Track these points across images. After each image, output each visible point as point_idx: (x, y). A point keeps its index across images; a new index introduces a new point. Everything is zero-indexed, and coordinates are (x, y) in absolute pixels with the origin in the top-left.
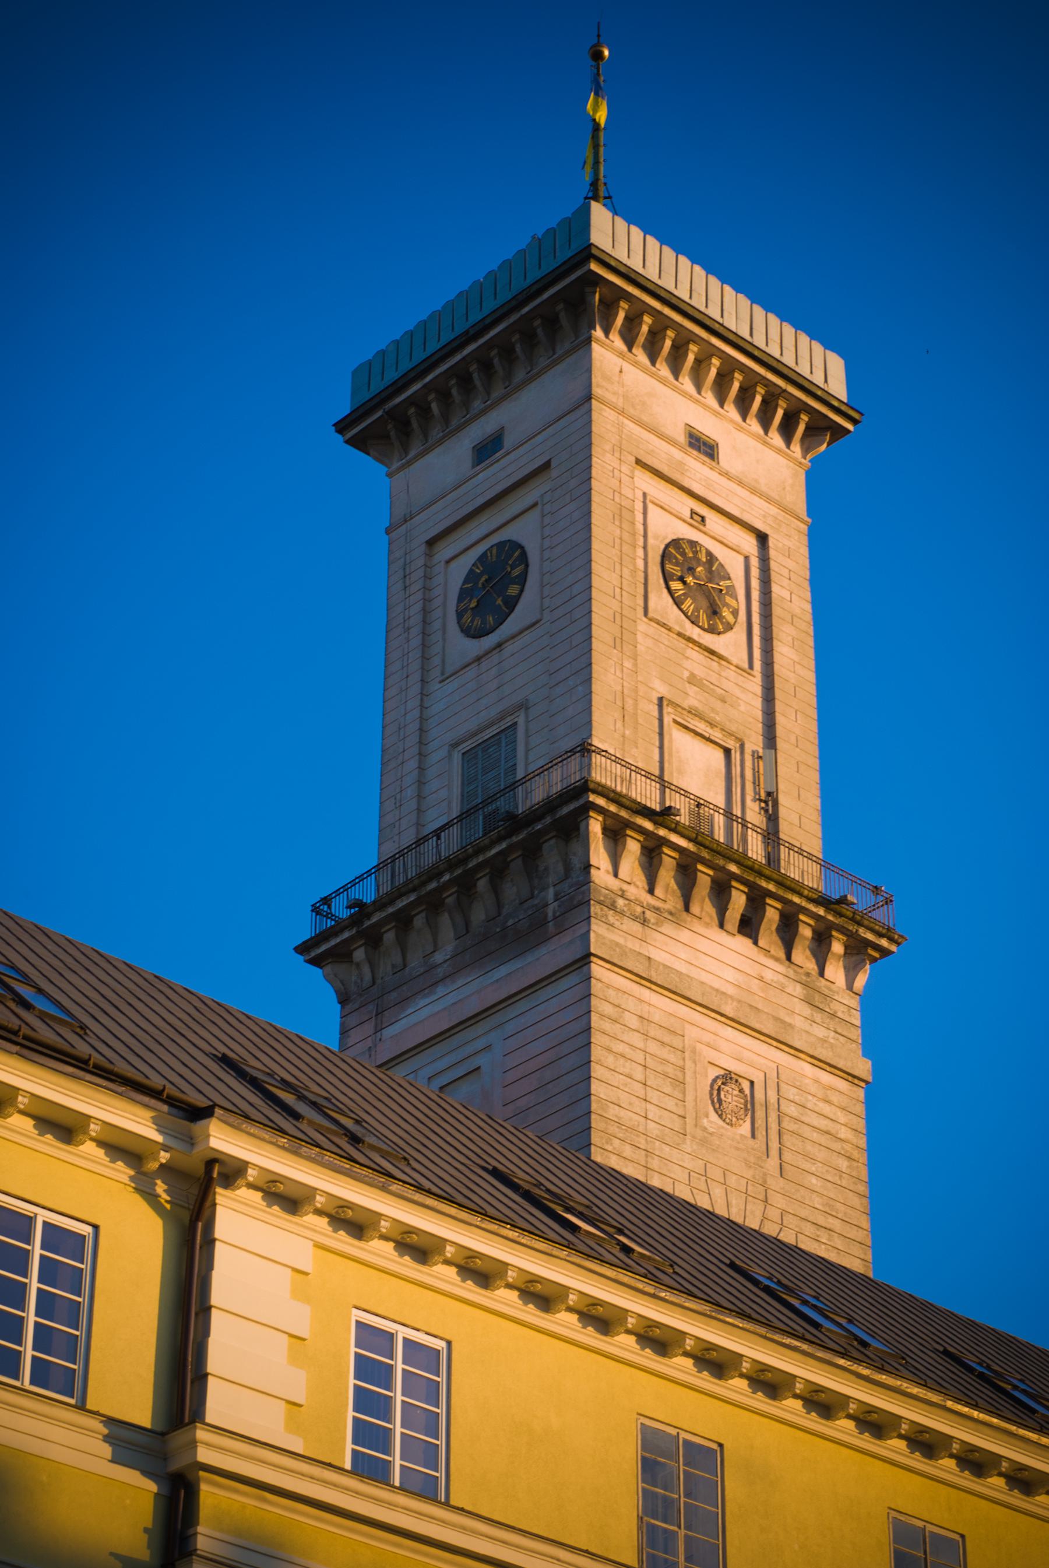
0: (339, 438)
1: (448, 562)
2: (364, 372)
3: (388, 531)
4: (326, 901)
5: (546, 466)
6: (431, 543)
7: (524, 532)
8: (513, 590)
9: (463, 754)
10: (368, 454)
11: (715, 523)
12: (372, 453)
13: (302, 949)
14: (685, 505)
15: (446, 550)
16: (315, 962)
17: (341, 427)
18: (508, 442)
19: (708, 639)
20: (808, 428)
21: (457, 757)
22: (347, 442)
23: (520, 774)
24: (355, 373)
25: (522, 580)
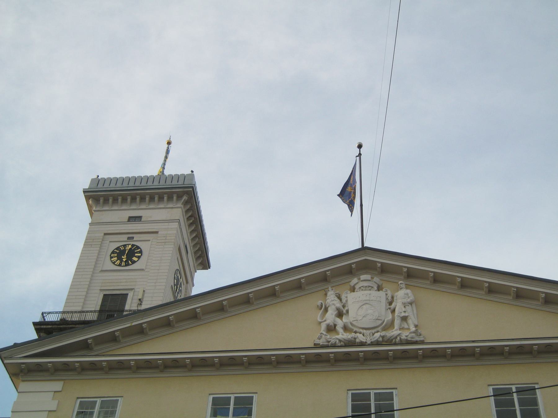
1: (110, 242)
2: (97, 181)
5: (157, 232)
6: (105, 234)
8: (135, 259)
9: (104, 295)
13: (35, 324)
17: (85, 192)
22: (85, 196)
24: (93, 180)
25: (139, 257)
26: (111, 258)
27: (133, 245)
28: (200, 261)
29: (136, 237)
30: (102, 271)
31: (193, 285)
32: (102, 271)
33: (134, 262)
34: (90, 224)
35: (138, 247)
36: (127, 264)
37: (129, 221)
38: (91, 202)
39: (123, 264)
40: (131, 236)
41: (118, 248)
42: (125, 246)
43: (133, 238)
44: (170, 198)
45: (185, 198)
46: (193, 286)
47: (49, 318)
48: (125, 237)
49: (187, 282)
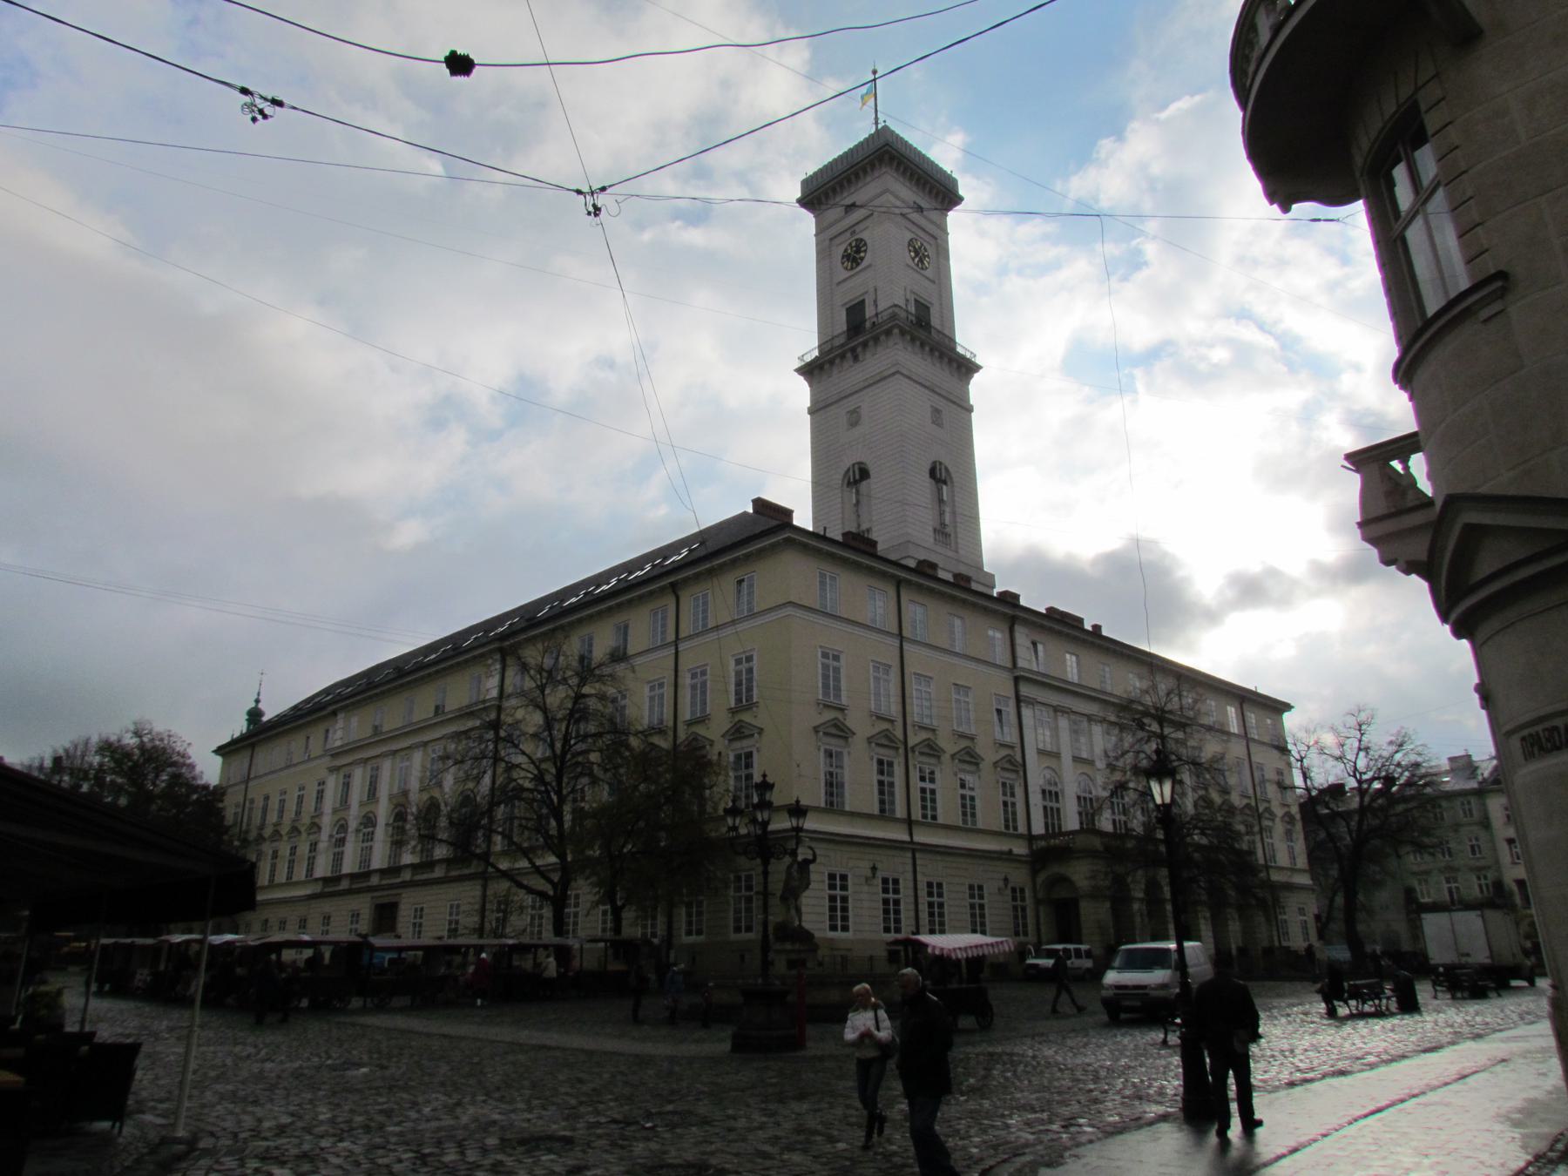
2: (806, 183)
6: (831, 239)
15: (838, 241)
19: (922, 272)
25: (865, 251)
26: (843, 263)
27: (857, 240)
29: (857, 229)
30: (839, 283)
32: (839, 283)
33: (862, 259)
34: (817, 235)
35: (862, 240)
36: (858, 264)
37: (846, 212)
40: (852, 229)
41: (846, 250)
42: (850, 244)
43: (854, 232)
44: (873, 167)
45: (887, 157)
47: (808, 359)
48: (848, 234)
49: (936, 239)
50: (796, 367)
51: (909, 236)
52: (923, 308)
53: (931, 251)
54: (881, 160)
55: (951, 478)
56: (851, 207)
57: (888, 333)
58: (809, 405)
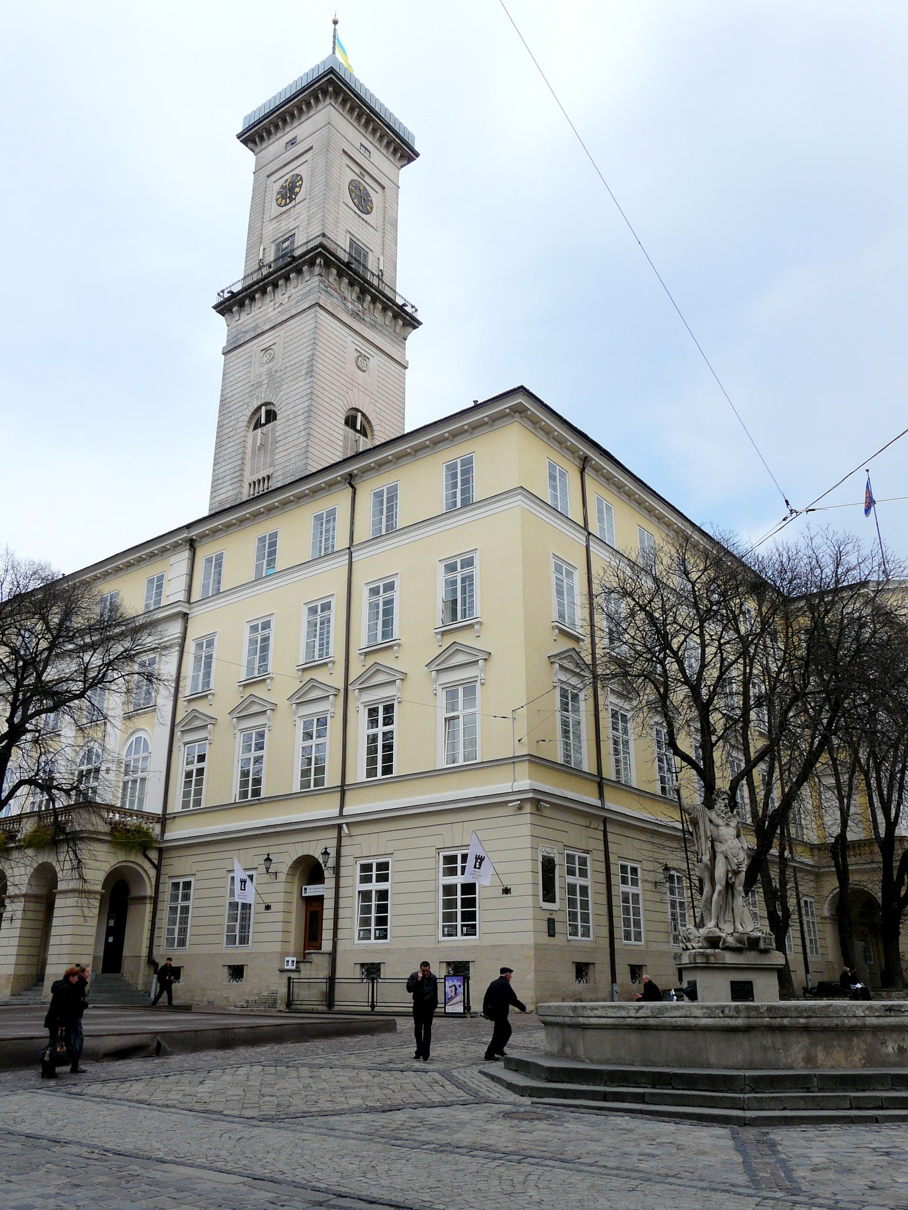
0: (238, 140)
3: (254, 173)
4: (223, 291)
5: (311, 148)
6: (268, 176)
7: (300, 171)
8: (297, 190)
10: (247, 146)
11: (367, 179)
12: (249, 145)
13: (215, 307)
14: (358, 170)
16: (220, 312)
17: (239, 137)
18: (298, 139)
20: (401, 156)
21: (273, 245)
23: (295, 246)
26: (277, 200)
28: (399, 154)
31: (399, 188)
33: (297, 193)
35: (298, 175)
38: (250, 145)
39: (288, 200)
44: (317, 100)
45: (330, 89)
46: (399, 188)
49: (384, 188)
50: (215, 303)
51: (350, 176)
52: (358, 252)
53: (376, 198)
54: (325, 93)
55: (372, 431)
56: (293, 142)
57: (312, 263)
58: (225, 345)
